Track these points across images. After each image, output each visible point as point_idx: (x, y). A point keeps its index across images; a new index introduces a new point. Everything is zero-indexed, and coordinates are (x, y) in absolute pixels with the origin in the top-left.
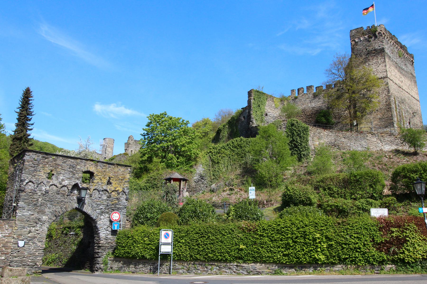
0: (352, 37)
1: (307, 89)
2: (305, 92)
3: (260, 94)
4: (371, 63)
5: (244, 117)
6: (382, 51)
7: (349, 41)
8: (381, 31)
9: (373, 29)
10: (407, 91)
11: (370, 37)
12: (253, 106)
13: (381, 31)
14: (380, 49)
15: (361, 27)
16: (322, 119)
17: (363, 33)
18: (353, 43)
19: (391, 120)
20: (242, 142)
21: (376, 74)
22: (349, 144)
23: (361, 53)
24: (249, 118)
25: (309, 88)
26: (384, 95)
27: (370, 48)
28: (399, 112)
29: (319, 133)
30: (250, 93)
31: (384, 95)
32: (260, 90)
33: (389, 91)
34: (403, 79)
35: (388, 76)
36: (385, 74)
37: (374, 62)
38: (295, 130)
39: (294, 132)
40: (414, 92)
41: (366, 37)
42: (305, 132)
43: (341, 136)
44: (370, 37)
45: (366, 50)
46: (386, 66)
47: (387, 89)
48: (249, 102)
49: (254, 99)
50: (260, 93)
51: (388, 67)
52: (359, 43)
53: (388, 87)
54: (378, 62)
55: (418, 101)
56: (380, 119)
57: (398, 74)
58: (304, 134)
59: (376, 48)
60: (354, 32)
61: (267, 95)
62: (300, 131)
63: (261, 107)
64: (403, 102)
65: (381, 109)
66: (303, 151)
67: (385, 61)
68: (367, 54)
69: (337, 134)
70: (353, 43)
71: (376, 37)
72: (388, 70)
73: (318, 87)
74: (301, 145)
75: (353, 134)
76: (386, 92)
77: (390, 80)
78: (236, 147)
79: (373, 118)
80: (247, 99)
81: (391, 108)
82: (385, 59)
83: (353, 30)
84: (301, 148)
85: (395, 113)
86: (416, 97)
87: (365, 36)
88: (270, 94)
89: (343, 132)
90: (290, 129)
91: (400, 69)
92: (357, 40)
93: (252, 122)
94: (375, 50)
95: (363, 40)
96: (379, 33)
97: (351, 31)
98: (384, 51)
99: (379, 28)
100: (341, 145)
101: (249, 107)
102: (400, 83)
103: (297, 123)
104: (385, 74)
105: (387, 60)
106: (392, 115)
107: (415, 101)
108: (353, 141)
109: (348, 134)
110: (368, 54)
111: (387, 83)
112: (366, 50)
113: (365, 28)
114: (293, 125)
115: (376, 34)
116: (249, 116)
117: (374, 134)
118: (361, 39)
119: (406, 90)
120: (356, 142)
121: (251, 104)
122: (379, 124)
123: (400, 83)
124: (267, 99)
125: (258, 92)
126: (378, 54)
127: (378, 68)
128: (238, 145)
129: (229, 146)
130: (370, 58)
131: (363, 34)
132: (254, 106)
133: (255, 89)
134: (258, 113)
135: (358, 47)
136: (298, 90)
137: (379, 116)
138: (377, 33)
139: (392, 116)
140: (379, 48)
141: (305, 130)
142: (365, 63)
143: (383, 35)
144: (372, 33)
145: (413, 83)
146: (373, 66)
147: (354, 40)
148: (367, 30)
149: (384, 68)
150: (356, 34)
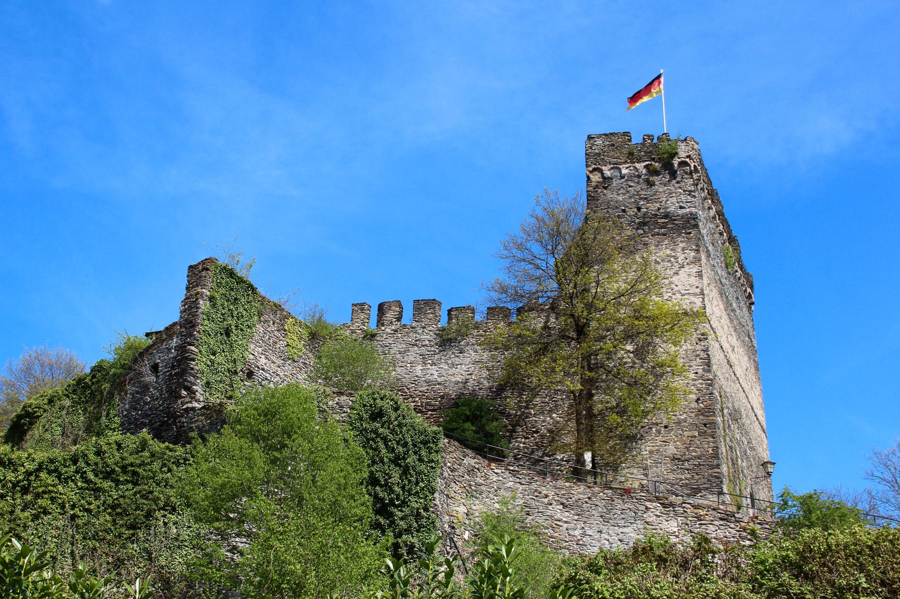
0: (594, 159)
1: (415, 309)
2: (407, 318)
3: (237, 284)
5: (155, 368)
6: (690, 223)
7: (584, 171)
8: (689, 157)
11: (652, 172)
12: (204, 325)
13: (689, 157)
14: (683, 217)
15: (626, 134)
16: (478, 425)
17: (631, 154)
18: (596, 178)
19: (712, 467)
20: (146, 454)
22: (577, 533)
23: (619, 216)
24: (180, 371)
25: (423, 307)
27: (653, 207)
29: (471, 471)
30: (197, 273)
31: (692, 376)
32: (240, 272)
33: (708, 363)
35: (708, 311)
38: (385, 440)
39: (381, 445)
41: (640, 166)
42: (423, 453)
43: (551, 494)
44: (652, 172)
45: (639, 209)
46: (700, 275)
47: (703, 355)
48: (190, 305)
49: (212, 299)
50: (240, 281)
51: (706, 280)
52: (615, 183)
53: (706, 350)
54: (676, 258)
56: (674, 459)
58: (420, 460)
59: (672, 209)
60: (599, 142)
62: (405, 445)
63: (233, 337)
65: (679, 423)
66: (408, 531)
67: (697, 260)
69: (534, 486)
70: (596, 178)
71: (673, 175)
72: (705, 292)
73: (457, 309)
74: (404, 503)
76: (697, 366)
77: (713, 329)
78: (108, 475)
79: (651, 452)
80: (182, 294)
81: (714, 424)
82: (698, 251)
84: (402, 519)
87: (637, 165)
88: (274, 299)
89: (560, 483)
90: (363, 432)
91: (728, 305)
93: (188, 389)
94: (666, 216)
95: (630, 177)
96: (683, 164)
97: (590, 138)
98: (696, 226)
101: (188, 324)
102: (730, 352)
103: (396, 409)
104: (698, 301)
105: (703, 257)
106: (716, 449)
109: (579, 491)
110: (645, 224)
112: (639, 209)
113: (637, 139)
114: (377, 415)
115: (672, 165)
116: (181, 365)
117: (672, 505)
118: (624, 171)
119: (741, 380)
121: (195, 315)
122: (671, 476)
123: (730, 352)
124: (260, 314)
125: (231, 274)
126: (678, 230)
127: (675, 279)
128: (124, 468)
129: (81, 464)
131: (632, 157)
132: (208, 326)
133: (223, 261)
134: (219, 359)
135: (610, 195)
136: (381, 308)
137: (671, 449)
138: (676, 162)
139: (716, 455)
140: (681, 212)
141: (425, 443)
143: (695, 176)
144: (663, 159)
147: (601, 171)
148: (643, 144)
149: (693, 280)
150: (605, 151)
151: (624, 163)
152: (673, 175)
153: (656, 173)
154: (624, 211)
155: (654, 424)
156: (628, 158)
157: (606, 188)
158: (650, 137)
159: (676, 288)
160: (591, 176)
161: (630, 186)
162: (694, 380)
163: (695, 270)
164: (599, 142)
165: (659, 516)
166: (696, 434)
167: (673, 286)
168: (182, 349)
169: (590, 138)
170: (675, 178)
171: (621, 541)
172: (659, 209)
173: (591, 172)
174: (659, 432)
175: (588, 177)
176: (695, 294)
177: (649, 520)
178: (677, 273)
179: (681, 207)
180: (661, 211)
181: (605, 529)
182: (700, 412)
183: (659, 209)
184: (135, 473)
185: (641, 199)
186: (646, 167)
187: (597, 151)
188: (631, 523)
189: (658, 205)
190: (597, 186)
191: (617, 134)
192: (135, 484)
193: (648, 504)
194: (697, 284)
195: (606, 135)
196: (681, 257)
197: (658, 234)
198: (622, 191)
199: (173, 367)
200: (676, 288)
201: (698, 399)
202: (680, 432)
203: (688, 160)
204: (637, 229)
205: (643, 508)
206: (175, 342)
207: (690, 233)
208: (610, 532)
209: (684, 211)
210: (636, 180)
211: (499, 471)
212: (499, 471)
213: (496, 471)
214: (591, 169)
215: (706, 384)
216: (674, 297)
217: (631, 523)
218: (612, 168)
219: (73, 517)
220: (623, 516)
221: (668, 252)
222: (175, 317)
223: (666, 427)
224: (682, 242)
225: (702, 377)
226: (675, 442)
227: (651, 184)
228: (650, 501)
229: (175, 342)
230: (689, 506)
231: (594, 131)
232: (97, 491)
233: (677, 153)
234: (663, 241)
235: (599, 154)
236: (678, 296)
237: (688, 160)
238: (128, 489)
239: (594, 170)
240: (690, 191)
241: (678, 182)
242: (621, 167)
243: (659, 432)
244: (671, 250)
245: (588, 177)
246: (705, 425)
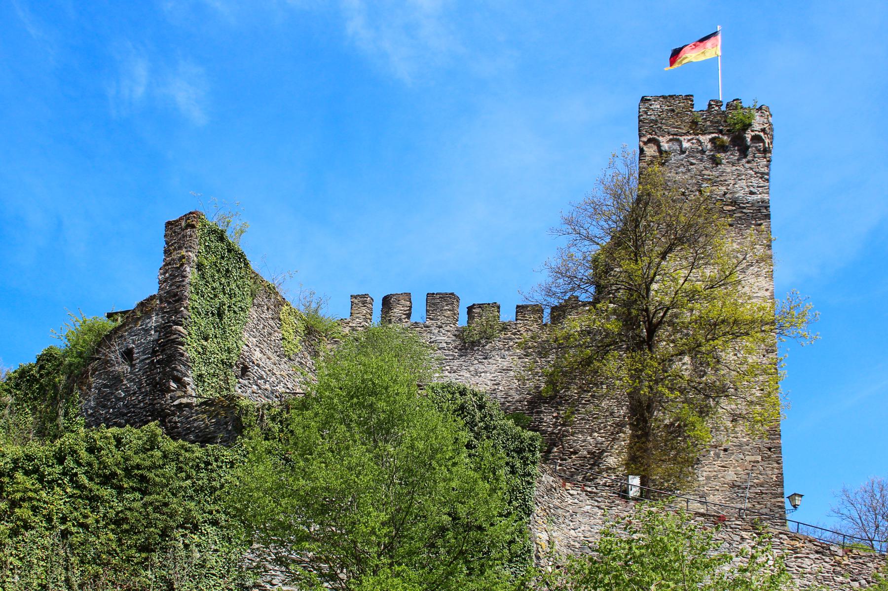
0: (649, 128)
8: (763, 130)
9: (737, 115)
13: (763, 130)
15: (689, 97)
18: (651, 150)
41: (705, 139)
52: (673, 159)
59: (740, 194)
60: (656, 106)
61: (256, 277)
71: (744, 151)
83: (657, 98)
87: (701, 138)
92: (665, 146)
94: (734, 202)
95: (692, 153)
96: (757, 139)
113: (700, 105)
118: (686, 145)
131: (695, 127)
138: (749, 136)
151: (685, 134)
152: (744, 151)
153: (723, 148)
158: (718, 103)
160: (645, 149)
161: (692, 164)
164: (656, 106)
168: (165, 329)
169: (644, 100)
170: (745, 156)
179: (752, 193)
180: (728, 196)
183: (725, 194)
184: (143, 479)
186: (712, 140)
187: (653, 117)
189: (724, 188)
190: (652, 162)
191: (677, 97)
192: (144, 493)
194: (766, 286)
195: (664, 97)
198: (682, 169)
199: (154, 353)
203: (762, 134)
206: (154, 321)
207: (760, 225)
209: (755, 197)
210: (699, 156)
211: (575, 492)
212: (575, 492)
213: (571, 492)
214: (645, 139)
218: (671, 140)
219: (65, 534)
222: (152, 288)
227: (716, 162)
229: (154, 321)
231: (649, 93)
232: (94, 500)
233: (750, 125)
237: (762, 134)
238: (135, 501)
239: (650, 141)
240: (762, 174)
241: (748, 162)
242: (681, 138)
245: (642, 151)
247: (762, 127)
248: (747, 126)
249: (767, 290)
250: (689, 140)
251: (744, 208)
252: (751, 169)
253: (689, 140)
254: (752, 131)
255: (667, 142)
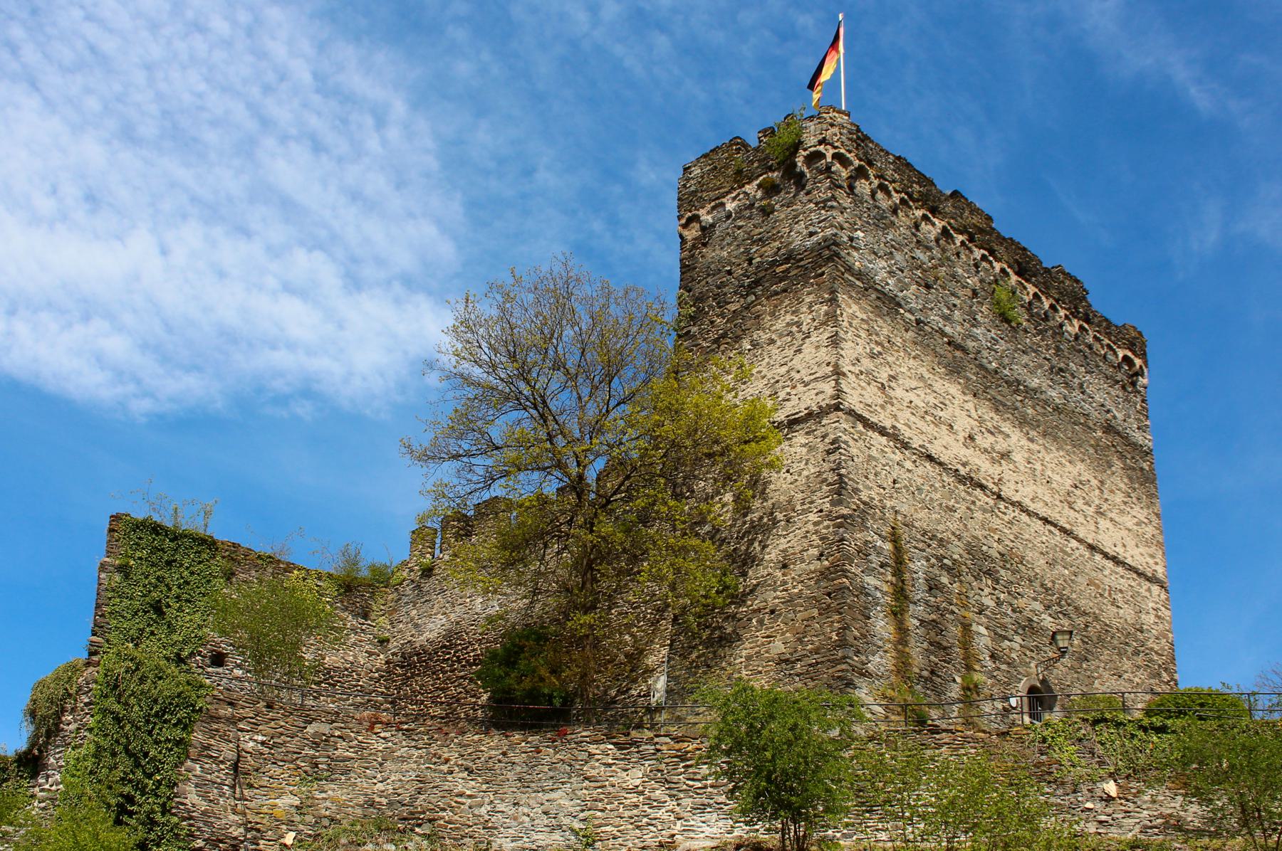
4: (764, 336)
10: (1043, 512)
14: (812, 250)
21: (782, 395)
26: (813, 517)
28: (933, 626)
31: (813, 517)
34: (1016, 439)
36: (828, 388)
37: (780, 325)
40: (1126, 529)
41: (750, 188)
44: (771, 189)
45: (750, 261)
54: (799, 324)
55: (1152, 579)
57: (964, 410)
64: (982, 565)
65: (790, 601)
67: (832, 318)
68: (751, 288)
70: (692, 233)
71: (800, 181)
75: (512, 746)
82: (833, 301)
85: (882, 626)
86: (1137, 555)
95: (739, 211)
96: (815, 157)
97: (686, 169)
99: (812, 126)
100: (447, 815)
107: (1112, 577)
108: (510, 788)
110: (757, 283)
111: (835, 446)
120: (523, 798)
127: (796, 363)
130: (765, 307)
137: (778, 647)
142: (738, 339)
145: (1118, 481)
146: (774, 350)
147: (695, 218)
154: (729, 272)
155: (754, 611)
156: (735, 181)
157: (705, 245)
159: (797, 376)
160: (686, 233)
161: (739, 227)
162: (816, 524)
163: (827, 335)
165: (610, 765)
166: (815, 612)
167: (793, 374)
170: (803, 187)
171: (545, 813)
172: (779, 249)
173: (685, 226)
174: (761, 622)
175: (681, 236)
176: (825, 377)
177: (594, 773)
178: (799, 351)
179: (811, 234)
180: (783, 251)
181: (523, 798)
182: (824, 574)
185: (753, 243)
186: (759, 186)
187: (693, 188)
188: (563, 783)
189: (777, 244)
193: (593, 748)
194: (828, 359)
195: (705, 156)
196: (806, 319)
197: (777, 293)
198: (728, 239)
200: (797, 376)
201: (821, 555)
202: (791, 615)
203: (821, 148)
204: (747, 295)
205: (584, 756)
207: (823, 274)
208: (532, 802)
209: (815, 239)
210: (747, 213)
214: (683, 221)
215: (835, 526)
216: (794, 392)
217: (563, 783)
218: (713, 208)
220: (551, 774)
221: (788, 318)
223: (772, 612)
224: (809, 294)
225: (828, 516)
226: (783, 634)
227: (766, 212)
228: (597, 742)
230: (667, 740)
233: (801, 143)
234: (782, 302)
235: (695, 192)
236: (800, 388)
240: (825, 201)
242: (724, 200)
243: (761, 622)
244: (794, 312)
245: (681, 236)
246: (829, 594)
247: (821, 137)
248: (797, 146)
249: (828, 364)
250: (734, 199)
251: (802, 259)
252: (810, 201)
253: (734, 199)
254: (805, 150)
255: (708, 213)
